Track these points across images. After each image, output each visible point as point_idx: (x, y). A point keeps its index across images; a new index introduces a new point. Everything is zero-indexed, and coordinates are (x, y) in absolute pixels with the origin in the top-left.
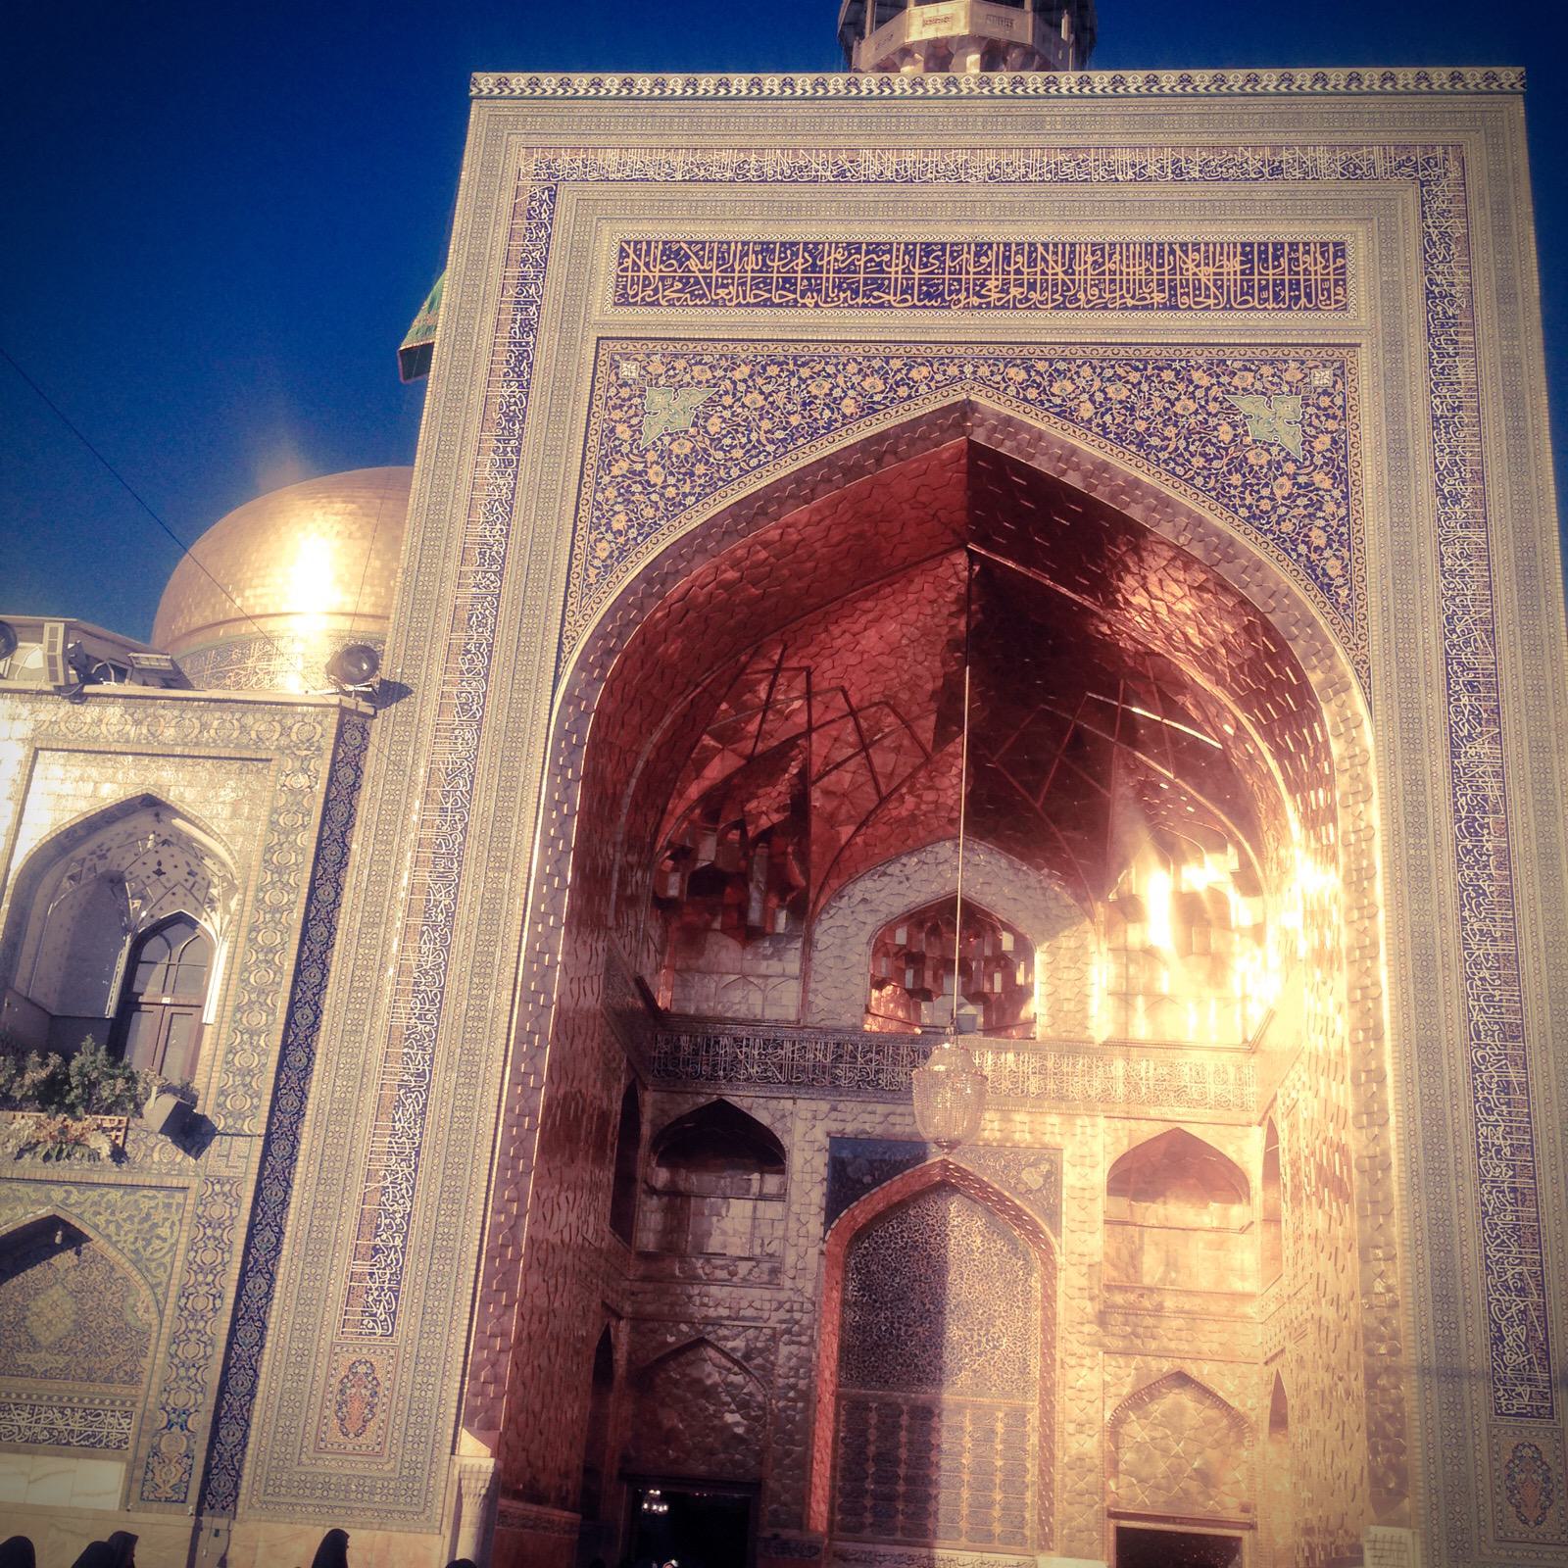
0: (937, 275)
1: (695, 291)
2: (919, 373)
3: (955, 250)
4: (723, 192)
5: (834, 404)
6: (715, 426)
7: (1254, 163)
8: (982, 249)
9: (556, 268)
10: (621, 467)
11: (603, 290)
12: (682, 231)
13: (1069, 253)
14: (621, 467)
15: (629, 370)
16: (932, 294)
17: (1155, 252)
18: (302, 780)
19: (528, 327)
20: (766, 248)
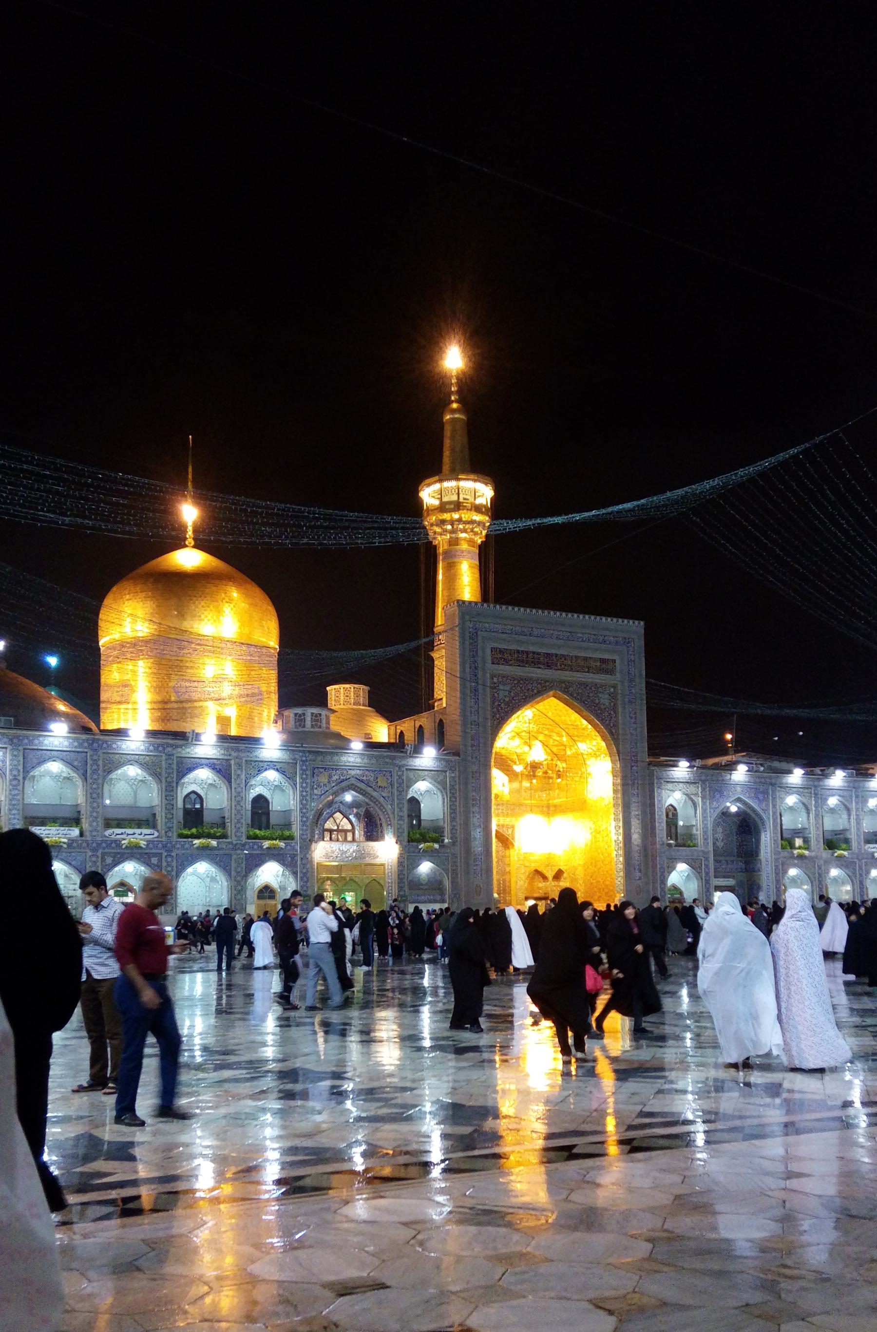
1: (506, 662)
2: (547, 684)
3: (552, 655)
5: (533, 691)
6: (512, 694)
7: (601, 638)
8: (556, 655)
9: (480, 653)
10: (496, 704)
11: (489, 659)
14: (496, 704)
15: (495, 680)
16: (549, 666)
17: (586, 659)
18: (453, 775)
19: (476, 668)
20: (518, 652)
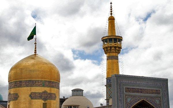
0: (141, 91)
1: (129, 91)
2: (141, 98)
4: (130, 84)
7: (156, 84)
11: (125, 91)
12: (128, 87)
13: (147, 90)
15: (126, 97)
16: (141, 92)
17: (152, 90)
